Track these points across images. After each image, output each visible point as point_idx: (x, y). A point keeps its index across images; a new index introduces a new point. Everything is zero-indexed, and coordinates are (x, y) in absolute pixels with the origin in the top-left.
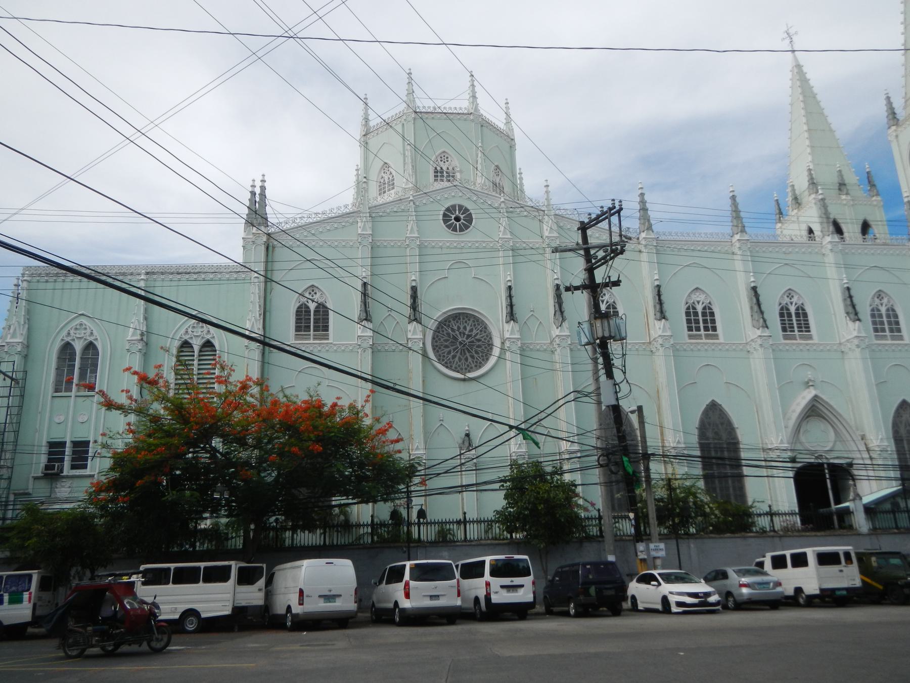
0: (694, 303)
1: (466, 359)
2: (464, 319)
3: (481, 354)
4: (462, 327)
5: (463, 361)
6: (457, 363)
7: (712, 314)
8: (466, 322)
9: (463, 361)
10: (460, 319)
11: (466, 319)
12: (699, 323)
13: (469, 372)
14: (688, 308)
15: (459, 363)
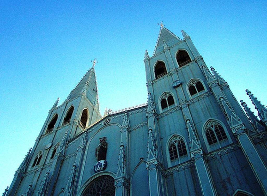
2: (101, 180)
8: (102, 182)
10: (99, 181)
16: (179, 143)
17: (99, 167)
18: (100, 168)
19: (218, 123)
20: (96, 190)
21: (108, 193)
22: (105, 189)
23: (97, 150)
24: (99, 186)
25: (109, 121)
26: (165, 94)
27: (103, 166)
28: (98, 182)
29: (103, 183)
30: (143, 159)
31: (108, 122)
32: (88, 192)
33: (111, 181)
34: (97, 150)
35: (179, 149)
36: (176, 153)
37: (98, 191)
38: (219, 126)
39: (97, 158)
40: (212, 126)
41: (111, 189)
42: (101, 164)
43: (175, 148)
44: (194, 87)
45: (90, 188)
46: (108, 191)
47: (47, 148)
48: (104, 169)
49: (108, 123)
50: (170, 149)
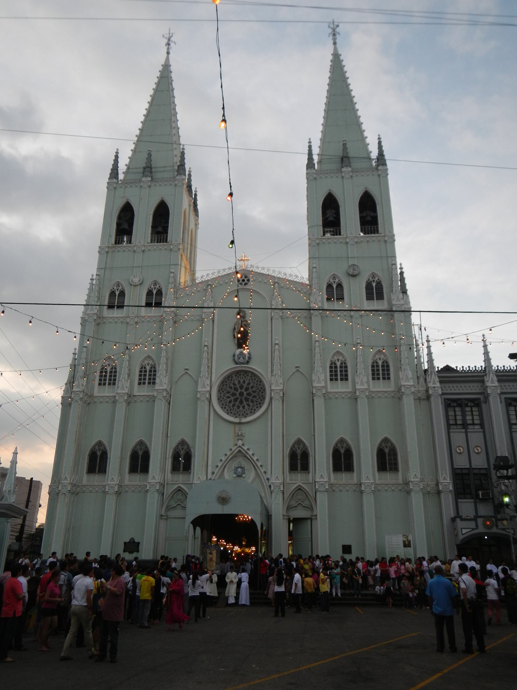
0: (377, 360)
1: (244, 407)
2: (243, 375)
3: (251, 407)
4: (242, 381)
5: (241, 408)
6: (236, 410)
7: (388, 366)
8: (245, 377)
9: (241, 408)
10: (240, 375)
11: (246, 375)
12: (382, 373)
13: (245, 417)
14: (373, 363)
15: (237, 410)
16: (342, 364)
17: (241, 358)
18: (243, 360)
19: (387, 359)
20: (238, 386)
21: (254, 394)
22: (250, 388)
23: (235, 329)
24: (242, 381)
25: (246, 280)
26: (334, 277)
27: (247, 358)
28: (238, 375)
29: (247, 379)
30: (298, 367)
31: (245, 282)
32: (226, 385)
33: (257, 381)
34: (235, 329)
35: (341, 371)
36: (336, 375)
37: (241, 387)
38: (387, 362)
39: (236, 342)
40: (380, 359)
41: (258, 391)
42: (245, 355)
43: (336, 367)
44: (372, 286)
45: (228, 380)
46: (254, 392)
47: (134, 284)
48: (248, 362)
49: (246, 284)
50: (331, 367)
